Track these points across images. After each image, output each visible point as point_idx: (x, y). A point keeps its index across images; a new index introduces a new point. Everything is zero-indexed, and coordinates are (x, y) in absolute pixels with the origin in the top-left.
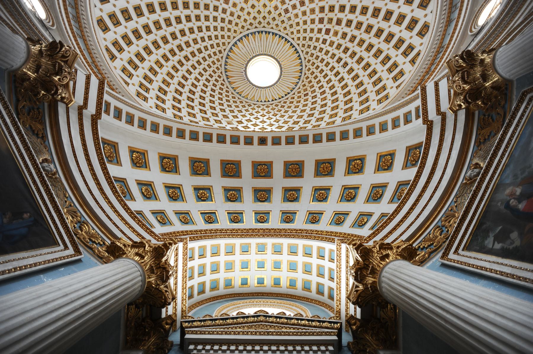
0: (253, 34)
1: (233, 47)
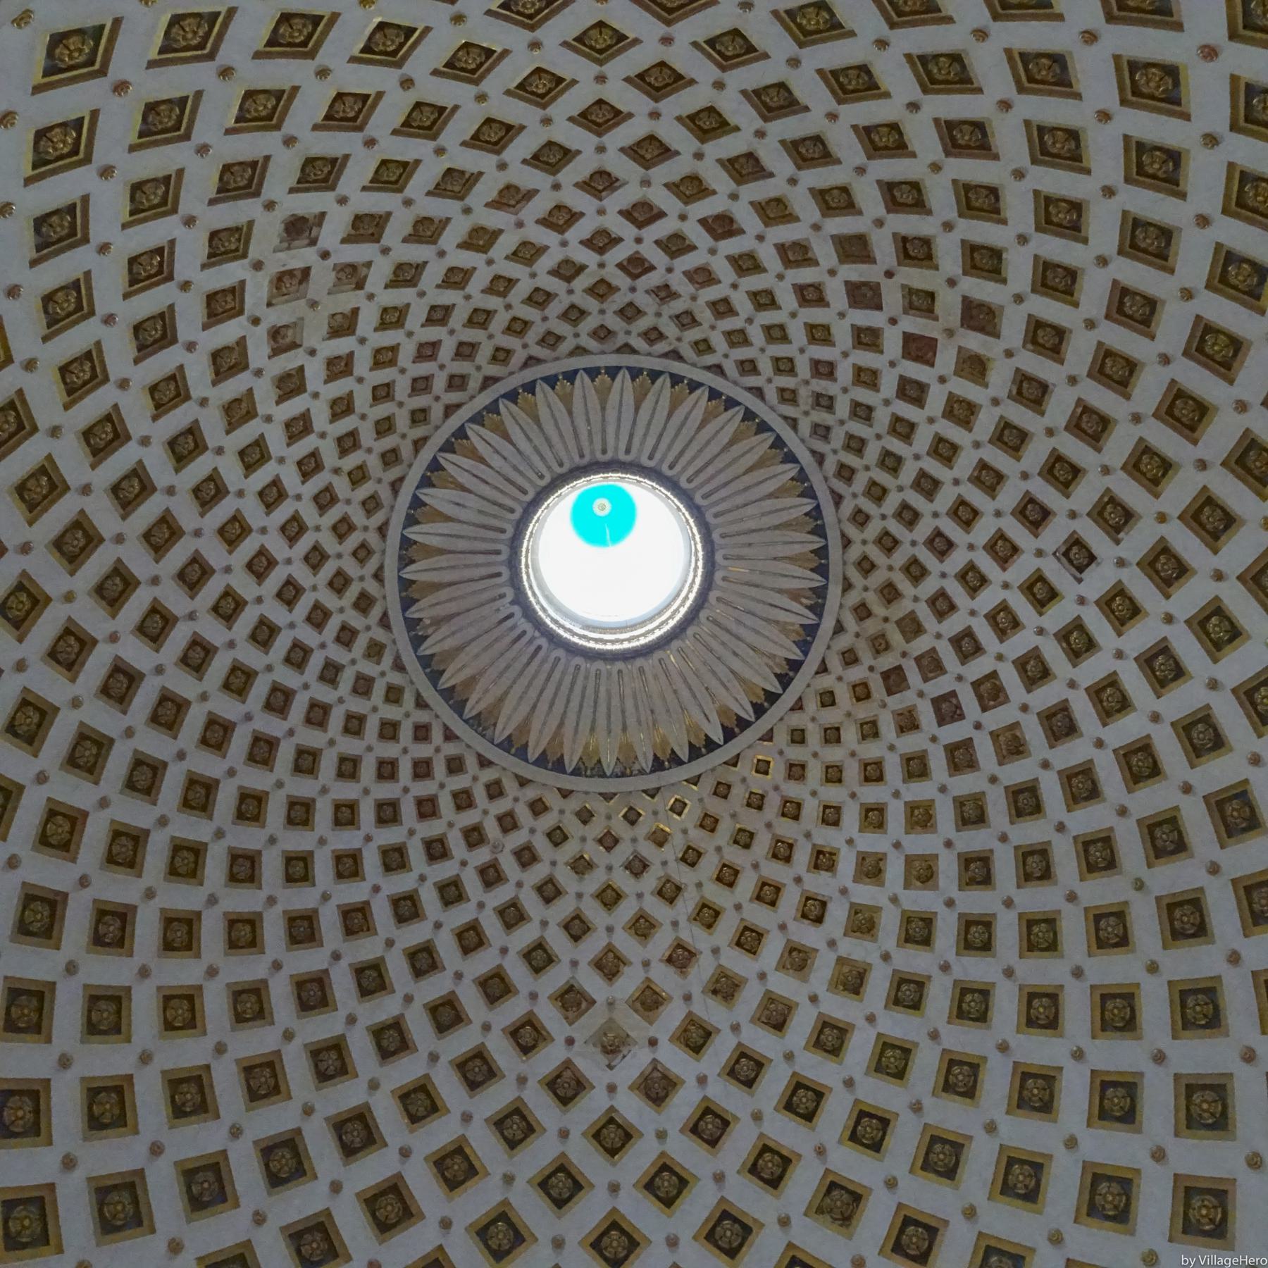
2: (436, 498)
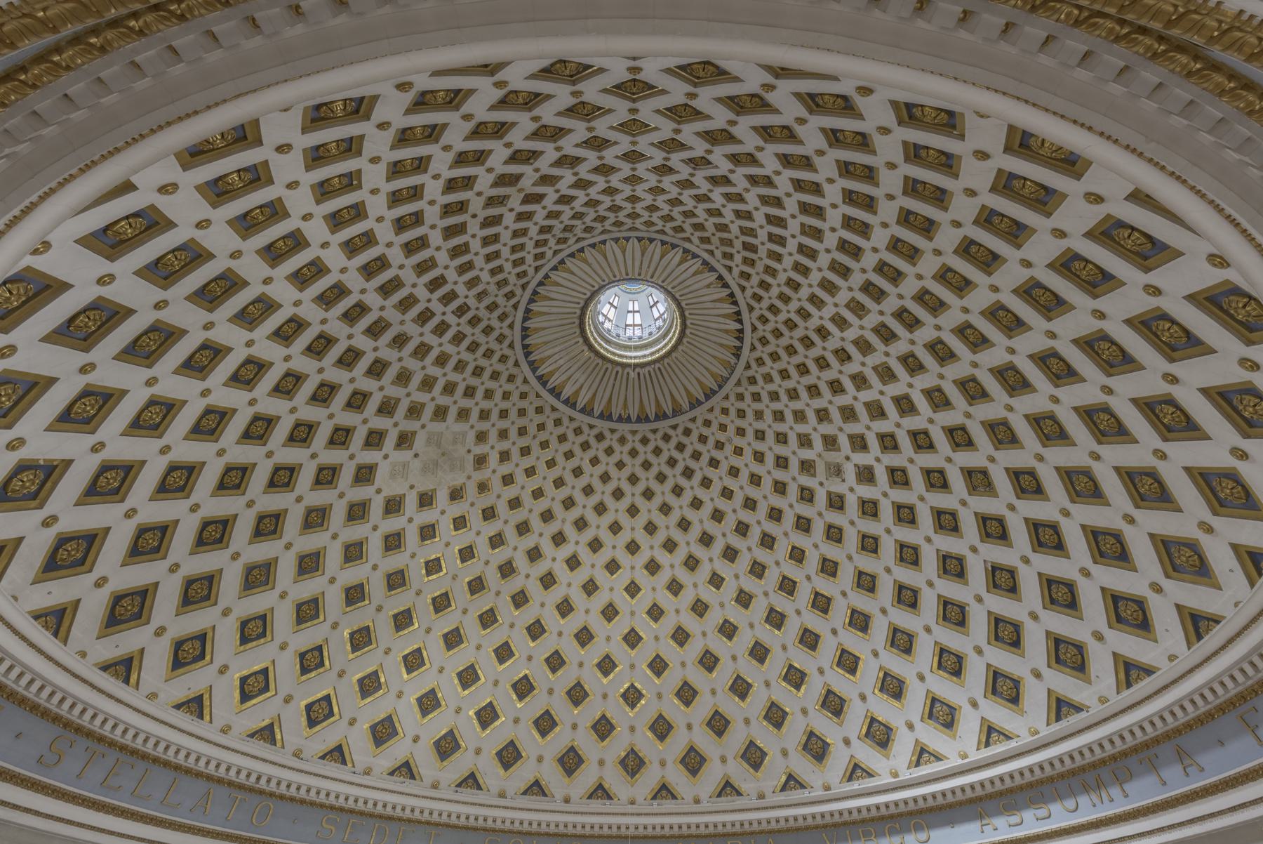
0: (533, 366)
1: (579, 406)
2: (567, 392)
